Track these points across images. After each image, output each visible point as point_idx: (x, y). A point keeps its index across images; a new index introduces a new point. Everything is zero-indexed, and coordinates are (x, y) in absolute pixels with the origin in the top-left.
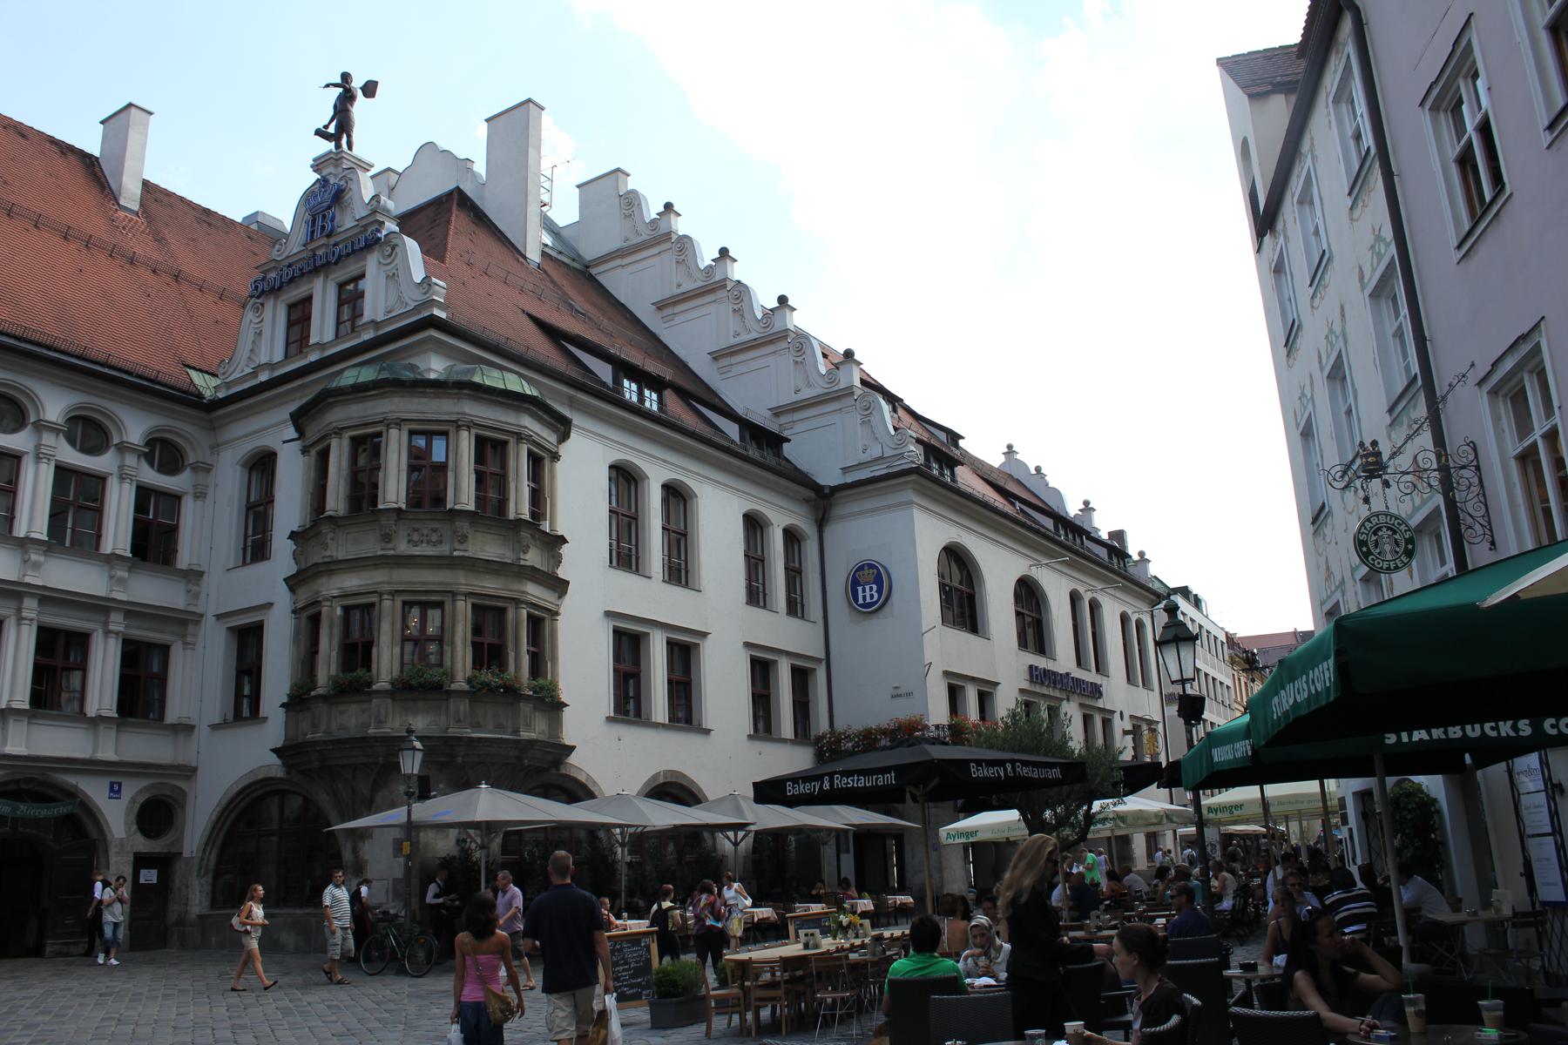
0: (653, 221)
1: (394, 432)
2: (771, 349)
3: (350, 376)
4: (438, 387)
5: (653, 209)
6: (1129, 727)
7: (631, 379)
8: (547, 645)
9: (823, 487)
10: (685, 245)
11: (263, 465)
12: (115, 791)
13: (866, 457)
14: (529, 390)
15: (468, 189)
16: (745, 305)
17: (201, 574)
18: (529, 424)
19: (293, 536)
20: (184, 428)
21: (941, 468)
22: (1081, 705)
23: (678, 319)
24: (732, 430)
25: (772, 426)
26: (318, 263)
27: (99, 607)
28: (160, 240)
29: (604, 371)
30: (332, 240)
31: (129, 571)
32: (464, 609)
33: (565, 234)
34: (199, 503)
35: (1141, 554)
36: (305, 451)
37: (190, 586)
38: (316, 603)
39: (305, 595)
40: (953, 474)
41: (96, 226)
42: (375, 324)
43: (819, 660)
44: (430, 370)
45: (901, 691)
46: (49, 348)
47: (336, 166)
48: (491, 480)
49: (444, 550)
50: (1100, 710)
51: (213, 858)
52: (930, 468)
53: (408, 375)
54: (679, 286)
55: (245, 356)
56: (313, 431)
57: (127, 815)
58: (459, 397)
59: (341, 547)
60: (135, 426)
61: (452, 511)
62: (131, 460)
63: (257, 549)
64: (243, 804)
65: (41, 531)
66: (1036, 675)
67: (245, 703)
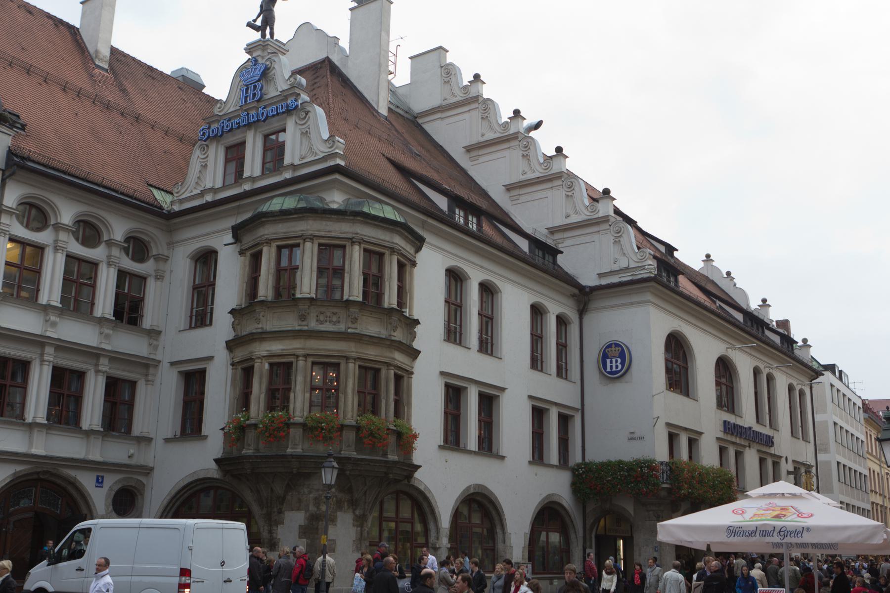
0: (466, 87)
2: (549, 185)
3: (276, 204)
4: (339, 214)
5: (467, 78)
6: (791, 469)
7: (460, 208)
8: (405, 396)
9: (584, 287)
10: (488, 107)
11: (206, 259)
12: (99, 482)
13: (616, 267)
14: (399, 219)
15: (335, 59)
17: (159, 333)
18: (399, 241)
19: (233, 312)
20: (150, 230)
21: (668, 276)
22: (758, 451)
23: (481, 159)
24: (524, 245)
25: (550, 242)
26: (251, 120)
27: (93, 354)
28: (123, 91)
29: (442, 203)
30: (262, 104)
31: (113, 329)
32: (352, 369)
33: (400, 92)
34: (159, 283)
35: (805, 341)
36: (242, 253)
37: (151, 341)
38: (251, 359)
40: (676, 281)
41: (80, 80)
42: (294, 167)
43: (577, 410)
44: (334, 202)
45: (636, 436)
46: (64, 172)
47: (263, 50)
48: (373, 283)
49: (342, 327)
50: (772, 455)
52: (661, 276)
53: (318, 204)
54: (483, 135)
56: (248, 239)
57: (106, 500)
59: (271, 322)
60: (119, 228)
61: (347, 301)
62: (116, 252)
63: (201, 316)
64: (186, 495)
65: (56, 301)
66: (729, 428)
67: (191, 423)
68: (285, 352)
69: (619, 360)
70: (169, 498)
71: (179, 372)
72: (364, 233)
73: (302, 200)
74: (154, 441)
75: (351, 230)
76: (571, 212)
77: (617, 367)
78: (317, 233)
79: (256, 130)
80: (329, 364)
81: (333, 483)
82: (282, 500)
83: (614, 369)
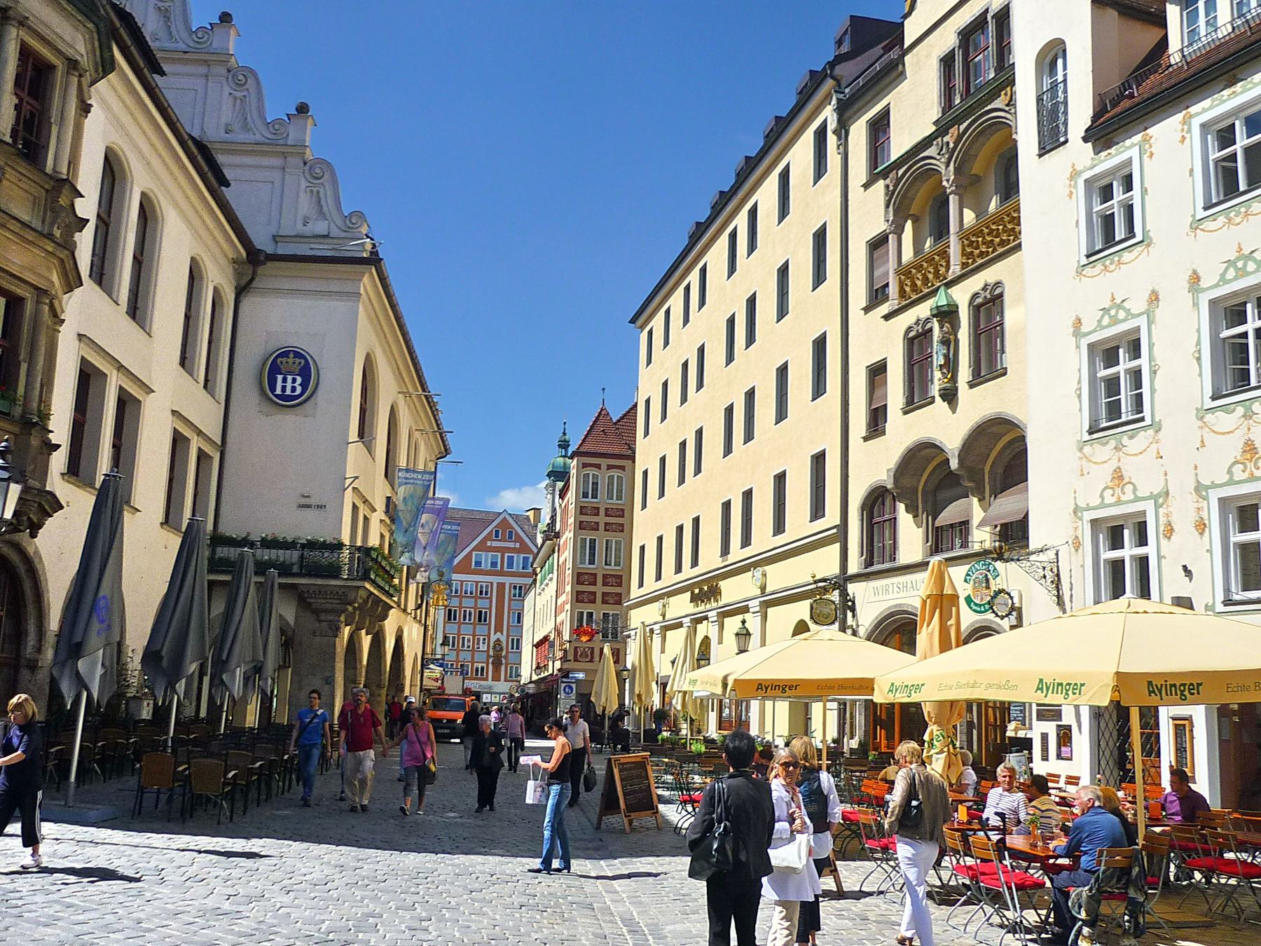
13: (308, 230)
69: (299, 380)
76: (236, 126)
77: (294, 389)
83: (288, 392)
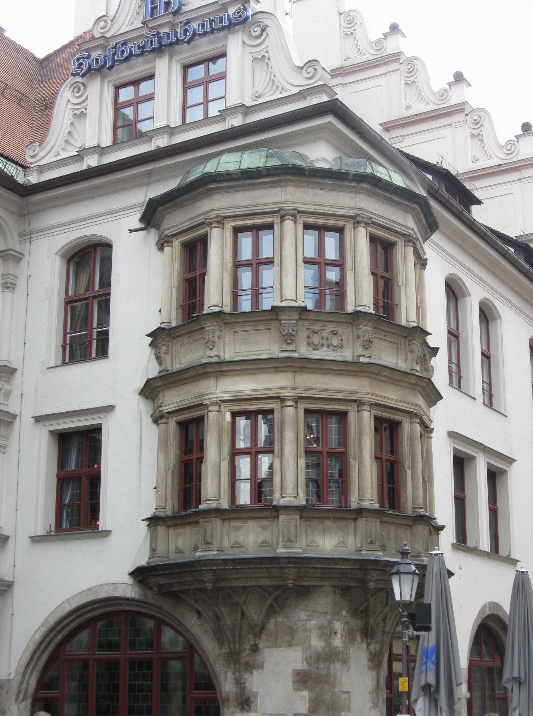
0: (378, 42)
1: (289, 224)
2: (515, 176)
16: (485, 132)
17: (13, 371)
26: (165, 42)
34: (8, 294)
39: (173, 399)
42: (246, 110)
44: (325, 160)
49: (347, 355)
51: (33, 682)
54: (408, 107)
55: (61, 141)
56: (177, 220)
58: (356, 191)
59: (232, 347)
68: (262, 394)
70: (44, 629)
71: (52, 432)
72: (370, 209)
73: (272, 156)
74: (11, 542)
75: (352, 204)
78: (302, 208)
79: (171, 57)
80: (325, 417)
81: (413, 600)
82: (259, 630)
